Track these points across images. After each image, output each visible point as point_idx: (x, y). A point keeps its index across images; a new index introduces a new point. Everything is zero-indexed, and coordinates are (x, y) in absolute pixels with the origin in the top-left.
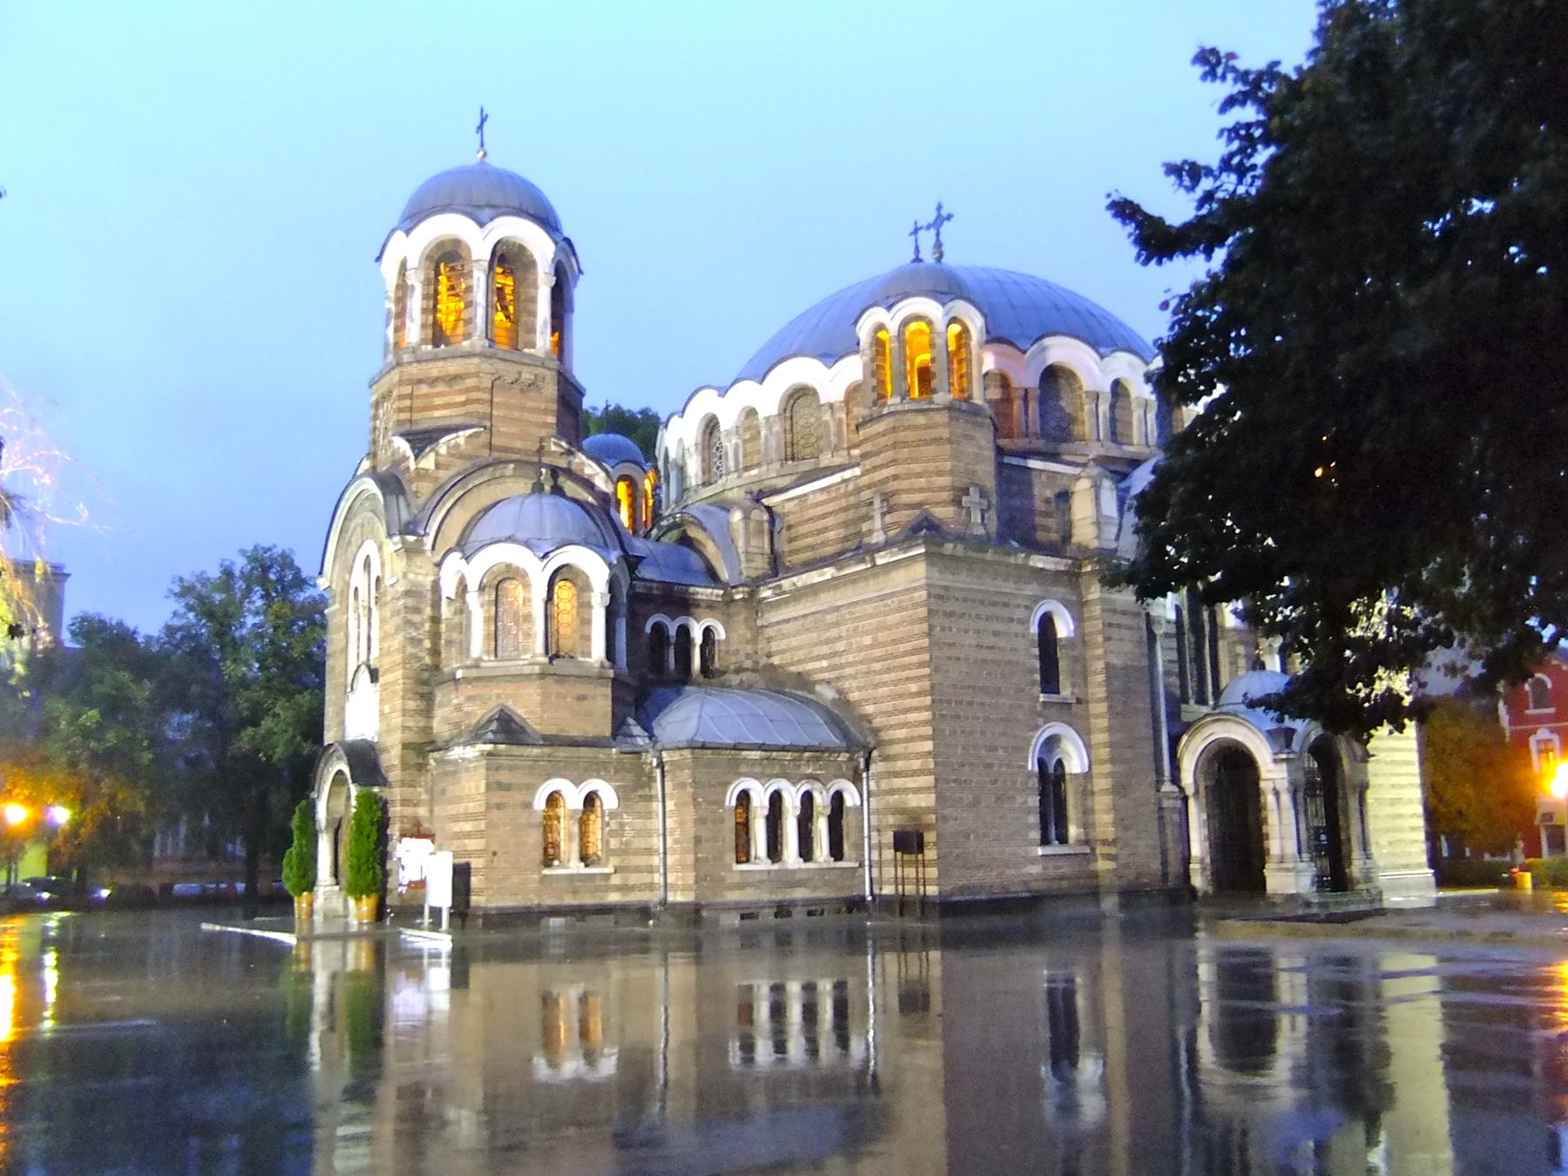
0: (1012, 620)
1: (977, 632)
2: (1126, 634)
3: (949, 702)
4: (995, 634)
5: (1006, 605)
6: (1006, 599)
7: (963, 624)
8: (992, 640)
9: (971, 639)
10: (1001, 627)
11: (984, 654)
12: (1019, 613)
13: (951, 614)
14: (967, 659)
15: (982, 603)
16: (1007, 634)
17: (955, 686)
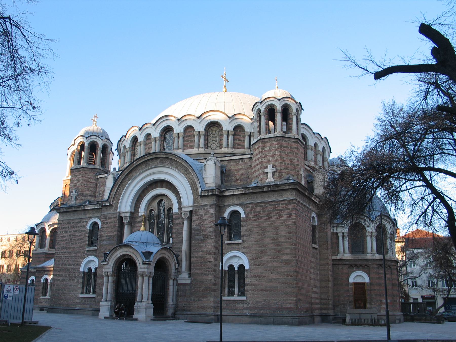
0: (81, 226)
1: (70, 232)
2: (109, 225)
3: (60, 252)
4: (75, 231)
5: (80, 222)
6: (80, 221)
7: (67, 230)
8: (73, 233)
9: (68, 234)
10: (77, 229)
11: (72, 238)
12: (84, 224)
13: (64, 228)
14: (66, 240)
15: (73, 223)
16: (79, 231)
17: (62, 248)
